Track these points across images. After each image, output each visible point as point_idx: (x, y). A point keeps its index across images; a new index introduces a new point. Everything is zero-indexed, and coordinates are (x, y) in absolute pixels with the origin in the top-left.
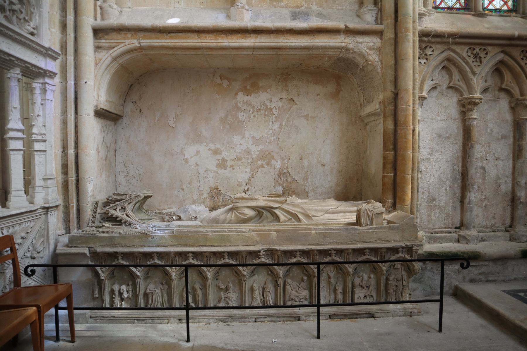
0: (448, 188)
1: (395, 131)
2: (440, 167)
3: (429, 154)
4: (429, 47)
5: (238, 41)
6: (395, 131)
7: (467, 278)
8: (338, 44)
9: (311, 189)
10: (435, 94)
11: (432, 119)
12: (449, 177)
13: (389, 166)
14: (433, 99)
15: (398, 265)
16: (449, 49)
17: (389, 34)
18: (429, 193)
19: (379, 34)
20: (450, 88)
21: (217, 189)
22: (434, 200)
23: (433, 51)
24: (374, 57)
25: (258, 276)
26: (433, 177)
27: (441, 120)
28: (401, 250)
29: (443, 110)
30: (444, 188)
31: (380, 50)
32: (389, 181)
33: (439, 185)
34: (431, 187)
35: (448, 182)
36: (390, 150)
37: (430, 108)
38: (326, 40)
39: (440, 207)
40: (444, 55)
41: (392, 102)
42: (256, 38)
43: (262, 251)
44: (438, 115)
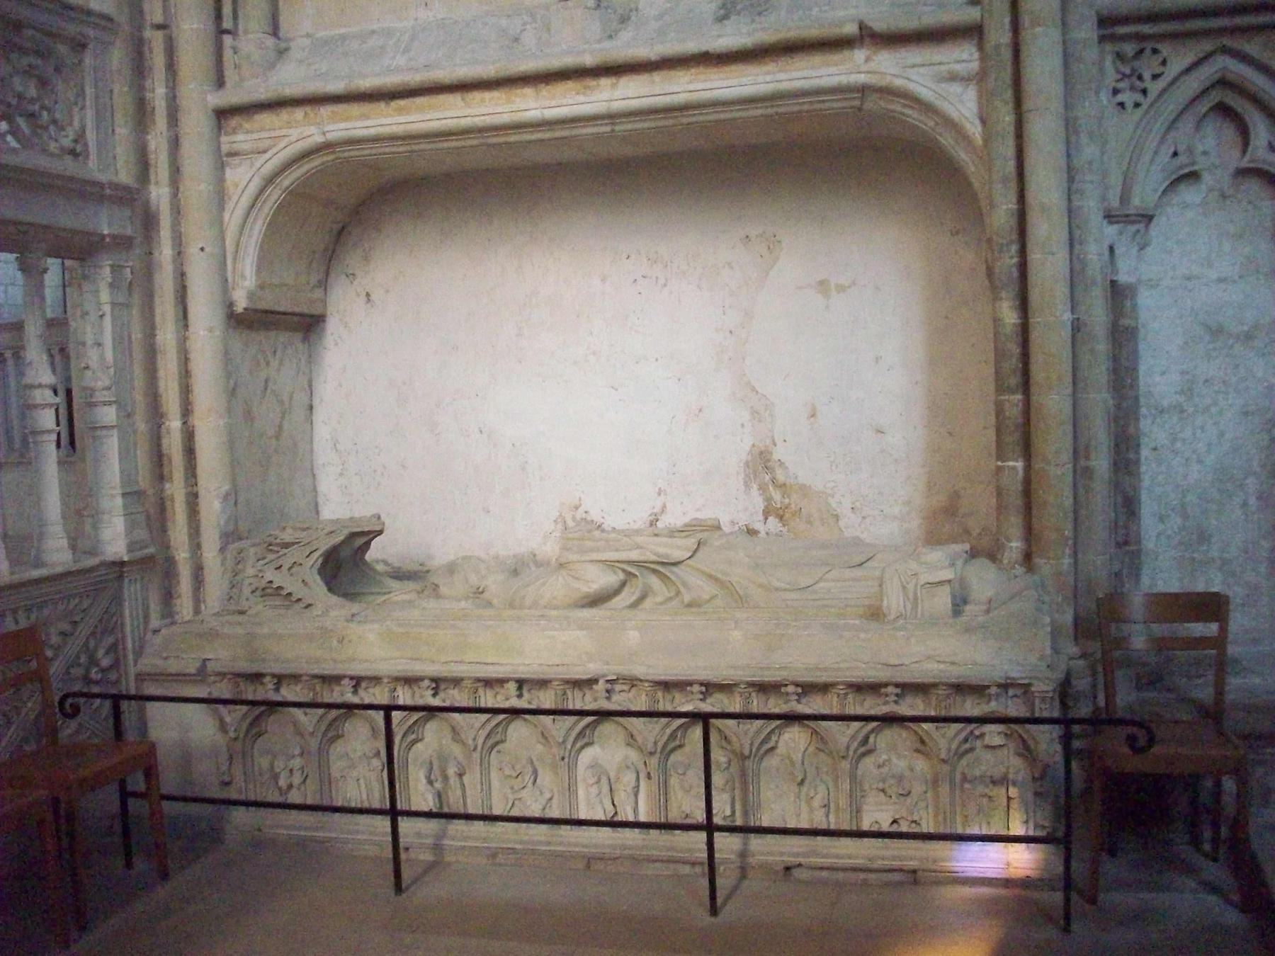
0: (1252, 501)
1: (1024, 330)
2: (1222, 434)
3: (1182, 392)
4: (1148, 52)
5: (564, 101)
6: (1024, 330)
7: (601, 686)
8: (844, 80)
9: (847, 503)
10: (1190, 194)
11: (1189, 279)
12: (1255, 463)
13: (1012, 438)
14: (1190, 214)
15: (993, 733)
16: (1225, 50)
17: (999, 36)
18: (1185, 516)
19: (974, 32)
20: (1242, 173)
21: (379, 518)
22: (1204, 537)
23: (1164, 63)
24: (962, 105)
25: (602, 748)
26: (1196, 467)
27: (1220, 280)
28: (993, 690)
29: (1227, 247)
30: (1238, 500)
31: (980, 77)
32: (1014, 484)
33: (1220, 491)
34: (1191, 498)
35: (1251, 482)
36: (1012, 391)
37: (1179, 242)
38: (805, 73)
39: (1225, 562)
40: (1207, 72)
41: (1012, 242)
42: (613, 86)
43: (601, 682)
44: (1210, 266)
